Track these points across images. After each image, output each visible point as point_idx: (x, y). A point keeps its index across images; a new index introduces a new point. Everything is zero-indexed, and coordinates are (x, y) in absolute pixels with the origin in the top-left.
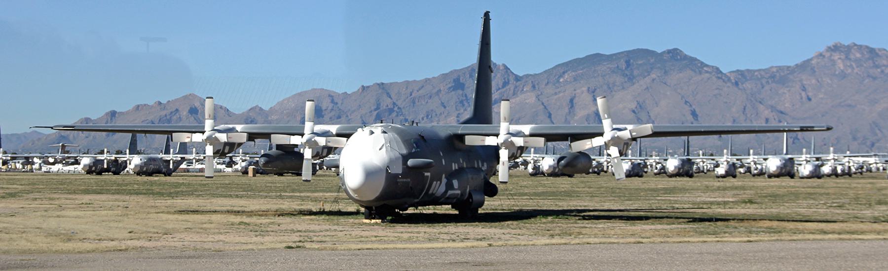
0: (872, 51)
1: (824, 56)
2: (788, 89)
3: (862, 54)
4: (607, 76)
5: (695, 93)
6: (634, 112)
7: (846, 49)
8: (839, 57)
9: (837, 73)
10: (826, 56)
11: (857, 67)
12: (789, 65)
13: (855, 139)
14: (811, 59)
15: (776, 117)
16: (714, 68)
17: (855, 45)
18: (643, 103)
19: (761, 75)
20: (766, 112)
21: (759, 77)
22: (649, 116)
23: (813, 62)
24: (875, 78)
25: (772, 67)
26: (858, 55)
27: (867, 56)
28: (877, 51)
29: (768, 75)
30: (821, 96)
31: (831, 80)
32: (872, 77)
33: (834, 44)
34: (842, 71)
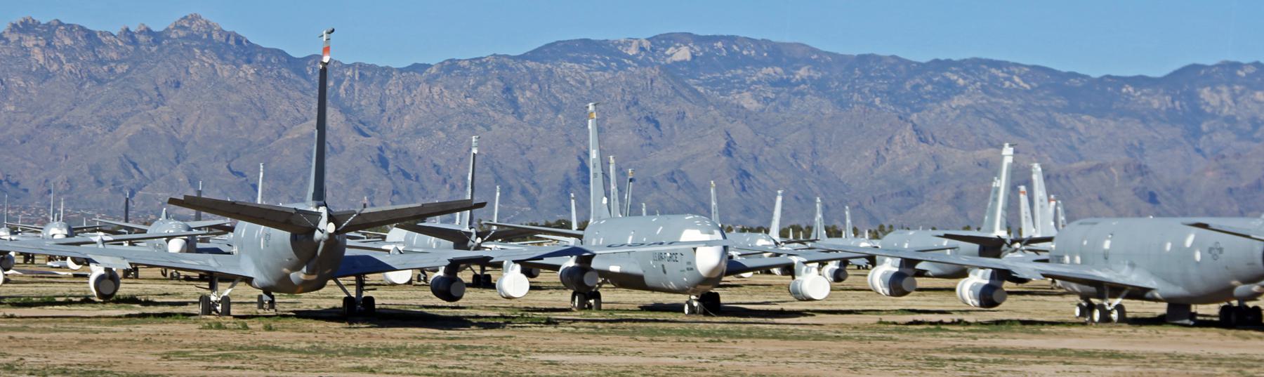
0: (90, 35)
1: (7, 41)
3: (74, 39)
7: (45, 30)
8: (35, 42)
9: (34, 69)
10: (12, 40)
11: (69, 61)
13: (100, 183)
17: (60, 24)
24: (100, 82)
26: (68, 41)
27: (83, 44)
28: (99, 36)
31: (25, 82)
32: (97, 80)
33: (23, 20)
34: (42, 67)
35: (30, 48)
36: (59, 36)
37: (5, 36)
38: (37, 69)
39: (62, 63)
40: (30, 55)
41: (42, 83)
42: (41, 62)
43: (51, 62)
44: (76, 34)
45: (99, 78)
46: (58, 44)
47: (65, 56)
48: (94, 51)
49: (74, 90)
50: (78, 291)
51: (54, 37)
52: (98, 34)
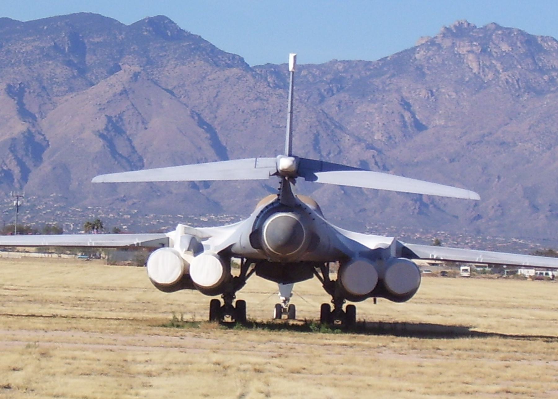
1: (439, 47)
2: (376, 105)
3: (512, 45)
4: (37, 65)
5: (215, 105)
6: (102, 136)
7: (481, 35)
8: (469, 48)
12: (367, 59)
13: (535, 208)
14: (414, 50)
15: (378, 159)
16: (236, 57)
17: (498, 27)
18: (117, 121)
19: (314, 76)
20: (357, 148)
21: (311, 79)
22: (133, 148)
23: (417, 56)
25: (336, 62)
26: (505, 47)
29: (329, 76)
30: (439, 122)
31: (457, 93)
33: (457, 25)
34: (477, 76)
35: (464, 55)
36: (496, 42)
37: (437, 42)
38: (471, 79)
39: (498, 72)
40: (463, 63)
41: (475, 94)
42: (475, 70)
43: (486, 69)
44: (515, 38)
45: (538, 88)
46: (495, 50)
47: (502, 64)
48: (533, 58)
49: (510, 103)
50: (36, 330)
51: (491, 43)
52: (539, 39)
